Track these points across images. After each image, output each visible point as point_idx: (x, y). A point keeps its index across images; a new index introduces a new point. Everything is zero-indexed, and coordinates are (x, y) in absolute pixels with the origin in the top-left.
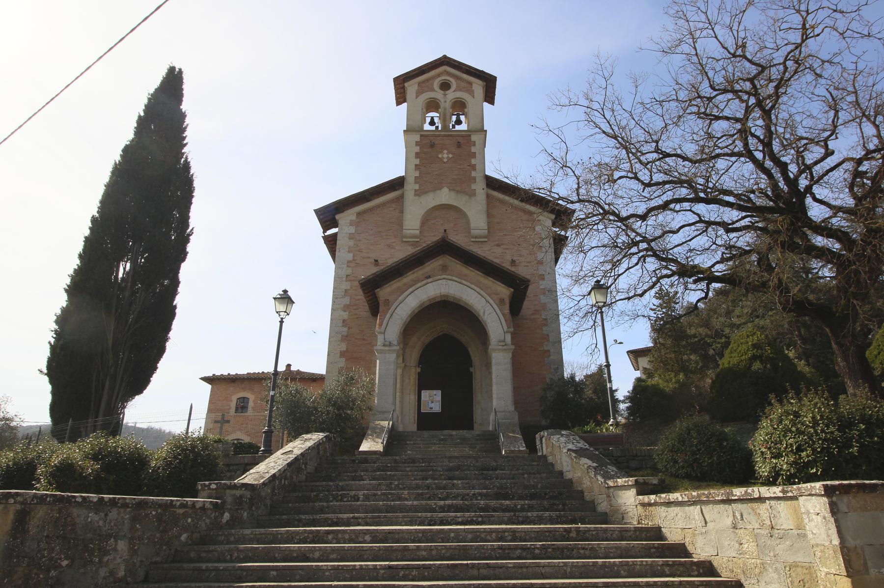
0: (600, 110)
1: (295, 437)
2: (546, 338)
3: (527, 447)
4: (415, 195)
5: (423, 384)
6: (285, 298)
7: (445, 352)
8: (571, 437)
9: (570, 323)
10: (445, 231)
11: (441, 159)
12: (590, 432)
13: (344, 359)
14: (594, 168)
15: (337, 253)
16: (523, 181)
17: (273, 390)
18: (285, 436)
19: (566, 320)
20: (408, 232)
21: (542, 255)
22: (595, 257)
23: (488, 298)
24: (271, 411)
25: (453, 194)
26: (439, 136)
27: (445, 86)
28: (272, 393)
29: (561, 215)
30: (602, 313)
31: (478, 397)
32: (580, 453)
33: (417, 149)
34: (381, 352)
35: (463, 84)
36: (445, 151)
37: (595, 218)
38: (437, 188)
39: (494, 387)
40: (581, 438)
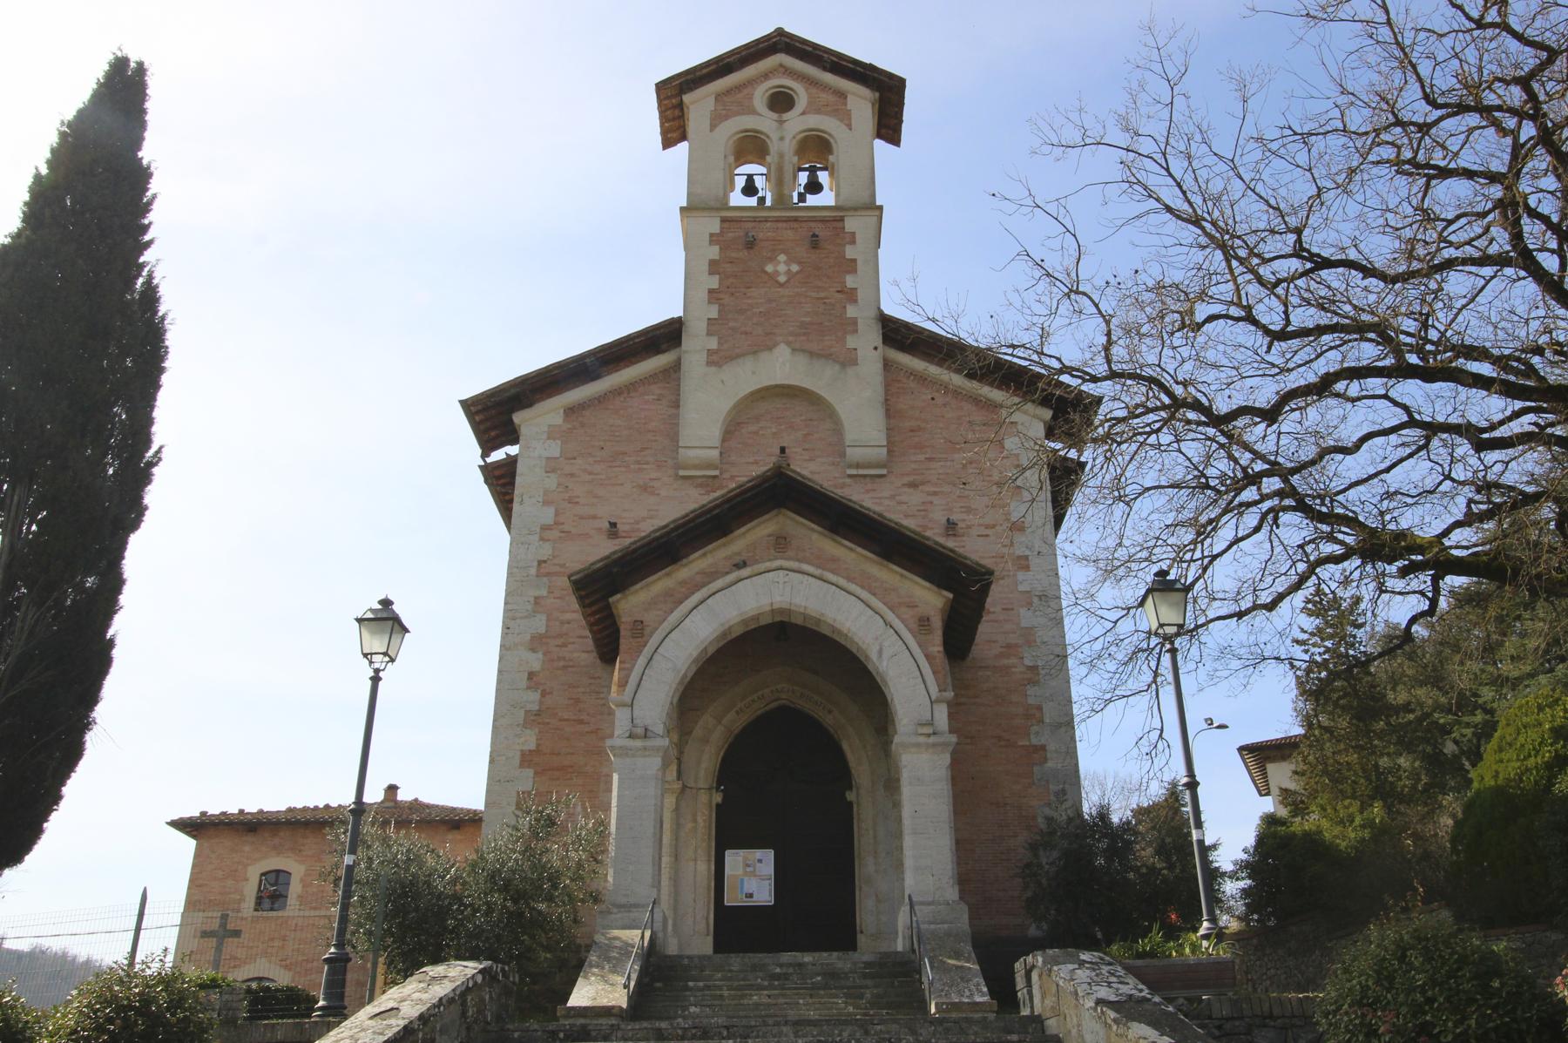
0: (1158, 157)
1: (407, 974)
2: (1034, 714)
3: (992, 993)
4: (709, 363)
5: (732, 831)
6: (386, 620)
7: (784, 749)
8: (1105, 969)
9: (1094, 678)
10: (783, 450)
11: (773, 277)
12: (1152, 955)
13: (530, 772)
14: (1147, 297)
15: (516, 507)
16: (975, 326)
17: (353, 851)
18: (381, 969)
19: (1084, 670)
20: (691, 453)
21: (1023, 508)
22: (1153, 512)
23: (890, 616)
24: (345, 907)
25: (802, 360)
26: (766, 220)
27: (781, 102)
28: (348, 859)
29: (1068, 410)
30: (1173, 651)
31: (867, 866)
32: (1128, 1009)
33: (714, 252)
34: (623, 752)
35: (825, 97)
36: (782, 258)
37: (1151, 417)
39: (908, 841)
40: (1129, 970)
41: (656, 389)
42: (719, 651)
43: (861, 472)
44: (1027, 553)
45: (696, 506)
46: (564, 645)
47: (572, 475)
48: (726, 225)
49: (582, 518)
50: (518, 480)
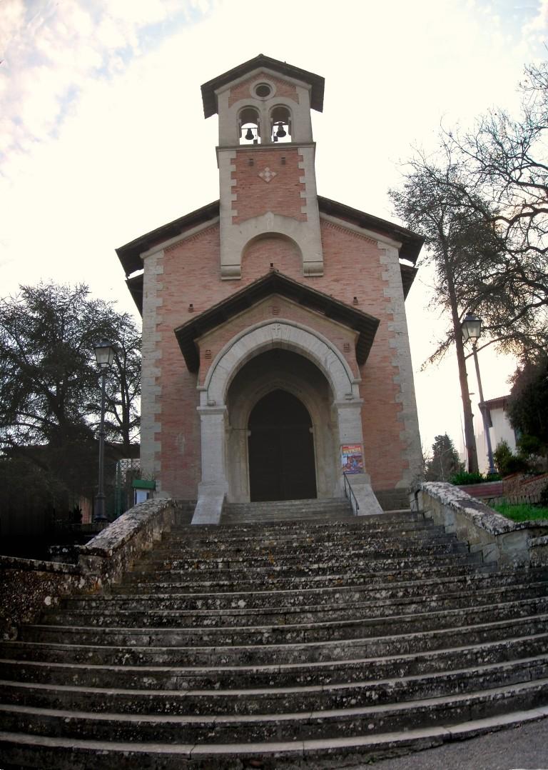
4: (234, 223)
11: (263, 179)
13: (160, 424)
15: (144, 300)
23: (331, 344)
27: (263, 91)
33: (233, 168)
34: (206, 412)
35: (285, 87)
36: (267, 169)
38: (259, 214)
41: (208, 237)
42: (248, 363)
43: (311, 275)
44: (392, 312)
45: (230, 294)
46: (171, 364)
47: (170, 282)
48: (239, 154)
49: (176, 303)
50: (144, 286)
